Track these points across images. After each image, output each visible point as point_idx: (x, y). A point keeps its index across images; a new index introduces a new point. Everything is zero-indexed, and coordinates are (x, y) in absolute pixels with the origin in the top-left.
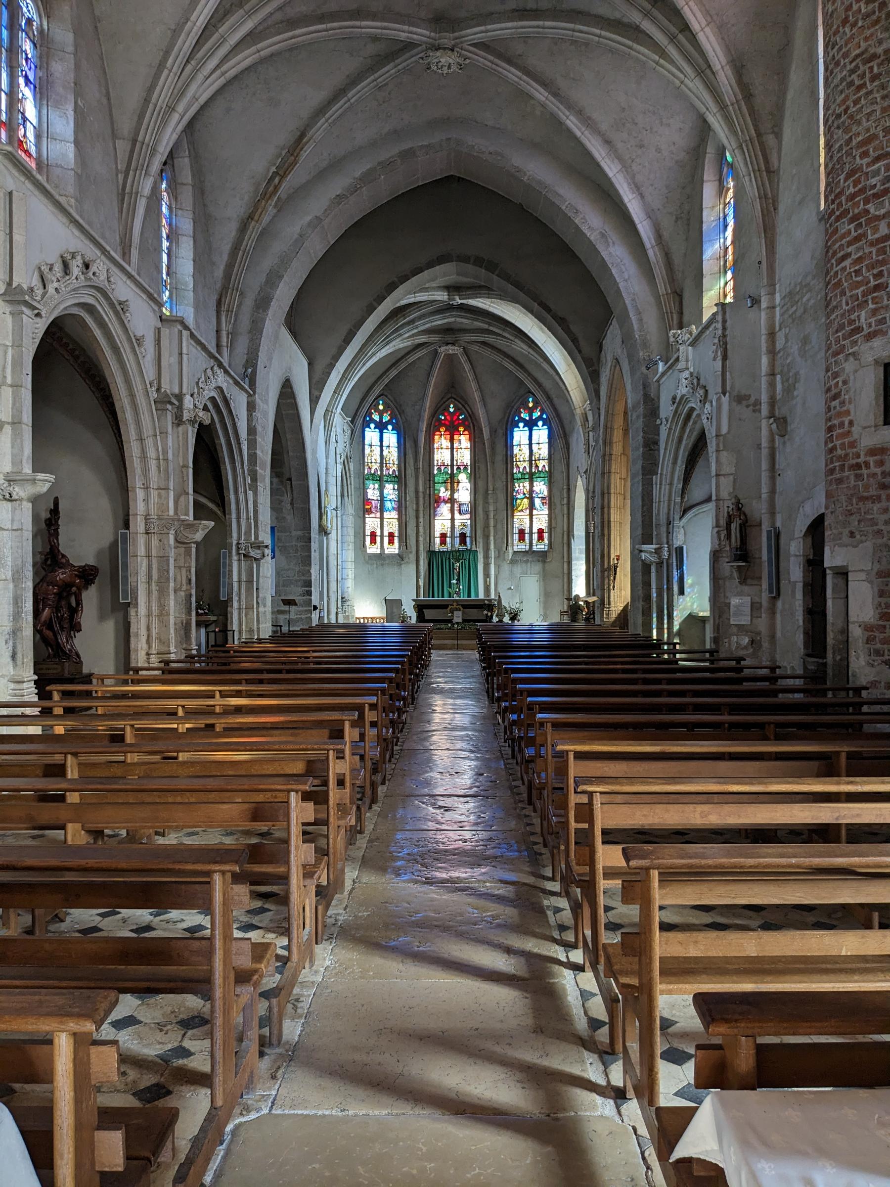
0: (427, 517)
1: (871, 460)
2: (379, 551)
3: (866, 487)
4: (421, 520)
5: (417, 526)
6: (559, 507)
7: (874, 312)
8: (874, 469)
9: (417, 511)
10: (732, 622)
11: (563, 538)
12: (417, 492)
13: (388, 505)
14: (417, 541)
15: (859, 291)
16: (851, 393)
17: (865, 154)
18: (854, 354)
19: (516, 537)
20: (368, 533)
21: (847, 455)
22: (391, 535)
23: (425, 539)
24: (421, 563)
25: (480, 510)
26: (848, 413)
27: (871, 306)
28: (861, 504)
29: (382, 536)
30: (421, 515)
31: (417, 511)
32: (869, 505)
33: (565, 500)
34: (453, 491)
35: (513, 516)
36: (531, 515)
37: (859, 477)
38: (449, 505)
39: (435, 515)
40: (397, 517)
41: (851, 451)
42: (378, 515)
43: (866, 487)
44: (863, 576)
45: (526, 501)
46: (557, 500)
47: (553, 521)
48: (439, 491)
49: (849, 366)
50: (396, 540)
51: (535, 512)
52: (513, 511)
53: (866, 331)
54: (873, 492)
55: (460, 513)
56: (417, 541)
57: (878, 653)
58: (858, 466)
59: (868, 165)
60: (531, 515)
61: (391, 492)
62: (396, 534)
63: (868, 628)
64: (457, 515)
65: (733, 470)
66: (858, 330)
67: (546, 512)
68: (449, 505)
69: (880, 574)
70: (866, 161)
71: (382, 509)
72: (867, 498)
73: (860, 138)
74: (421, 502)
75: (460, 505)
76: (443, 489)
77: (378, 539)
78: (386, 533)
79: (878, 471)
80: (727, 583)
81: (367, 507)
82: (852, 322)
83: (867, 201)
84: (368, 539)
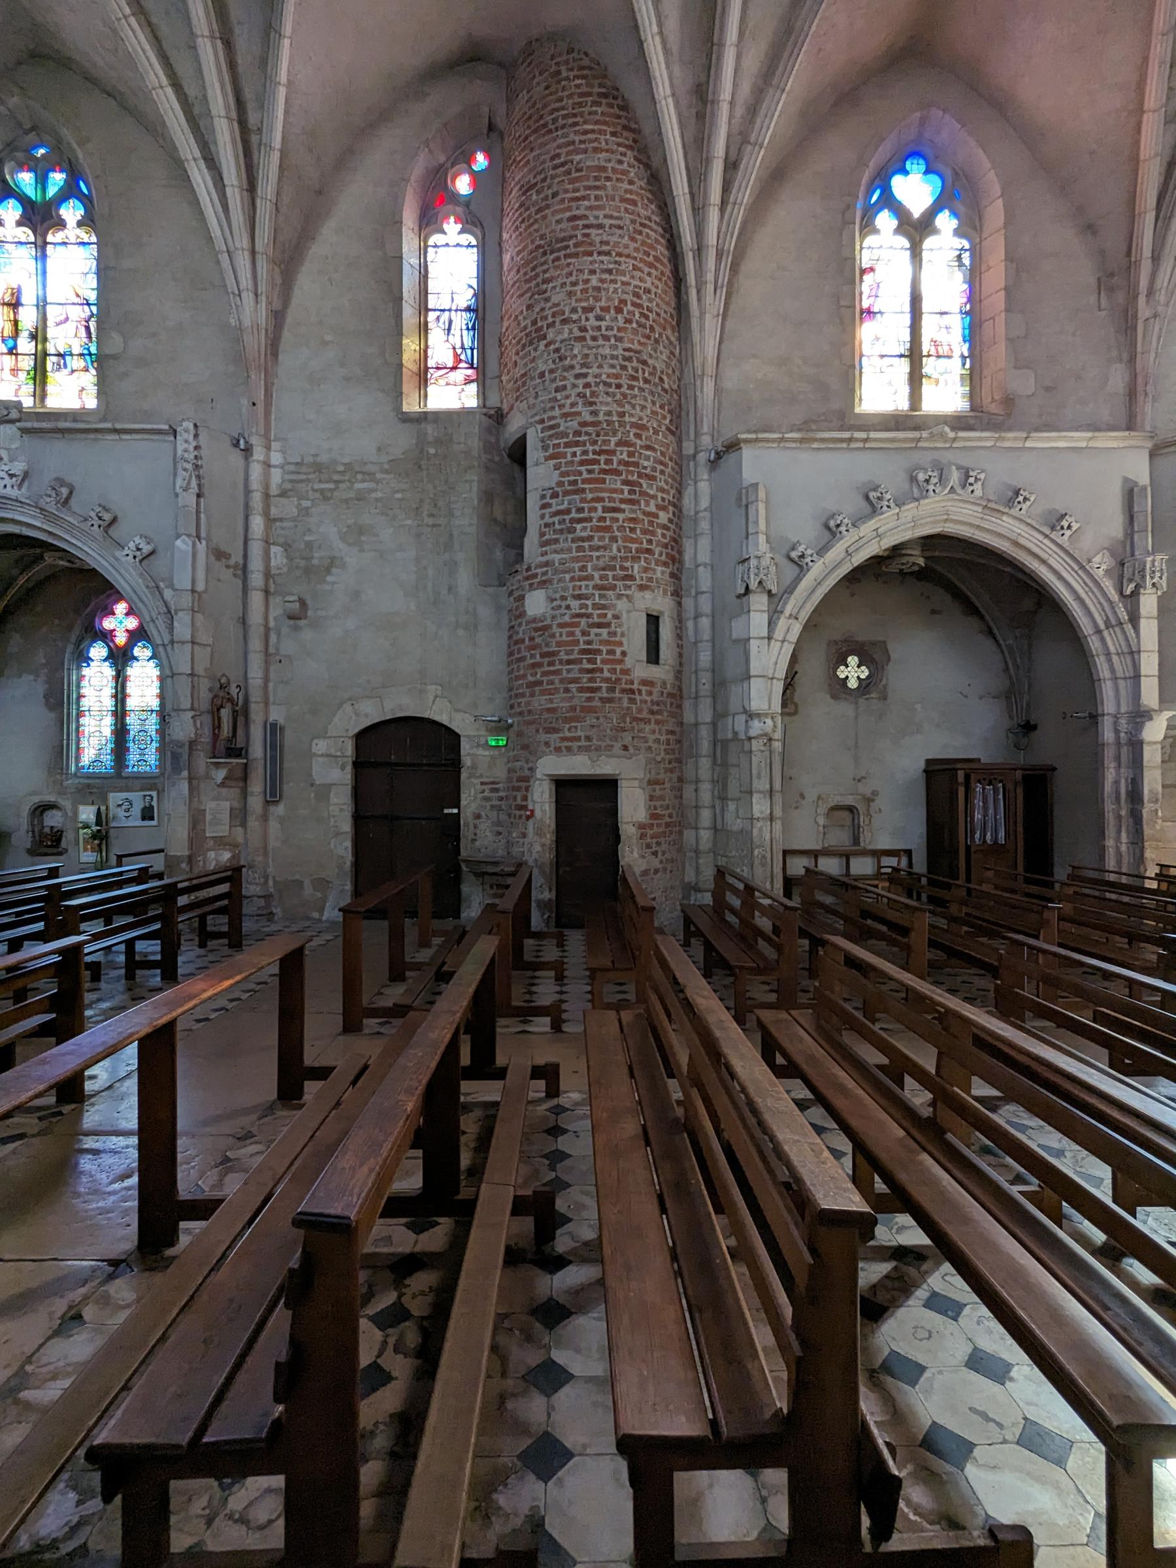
1: (644, 689)
3: (640, 711)
7: (646, 570)
8: (645, 697)
10: (208, 835)
15: (634, 546)
16: (625, 628)
17: (638, 436)
18: (627, 596)
21: (618, 680)
26: (621, 644)
27: (643, 563)
28: (634, 723)
32: (642, 725)
37: (632, 701)
41: (624, 678)
43: (640, 711)
44: (636, 783)
49: (622, 605)
53: (638, 582)
54: (645, 715)
57: (649, 846)
58: (632, 691)
59: (641, 447)
63: (641, 826)
65: (210, 641)
66: (631, 578)
69: (650, 783)
70: (639, 442)
72: (641, 720)
73: (633, 420)
79: (648, 699)
80: (202, 786)
82: (623, 568)
83: (640, 475)
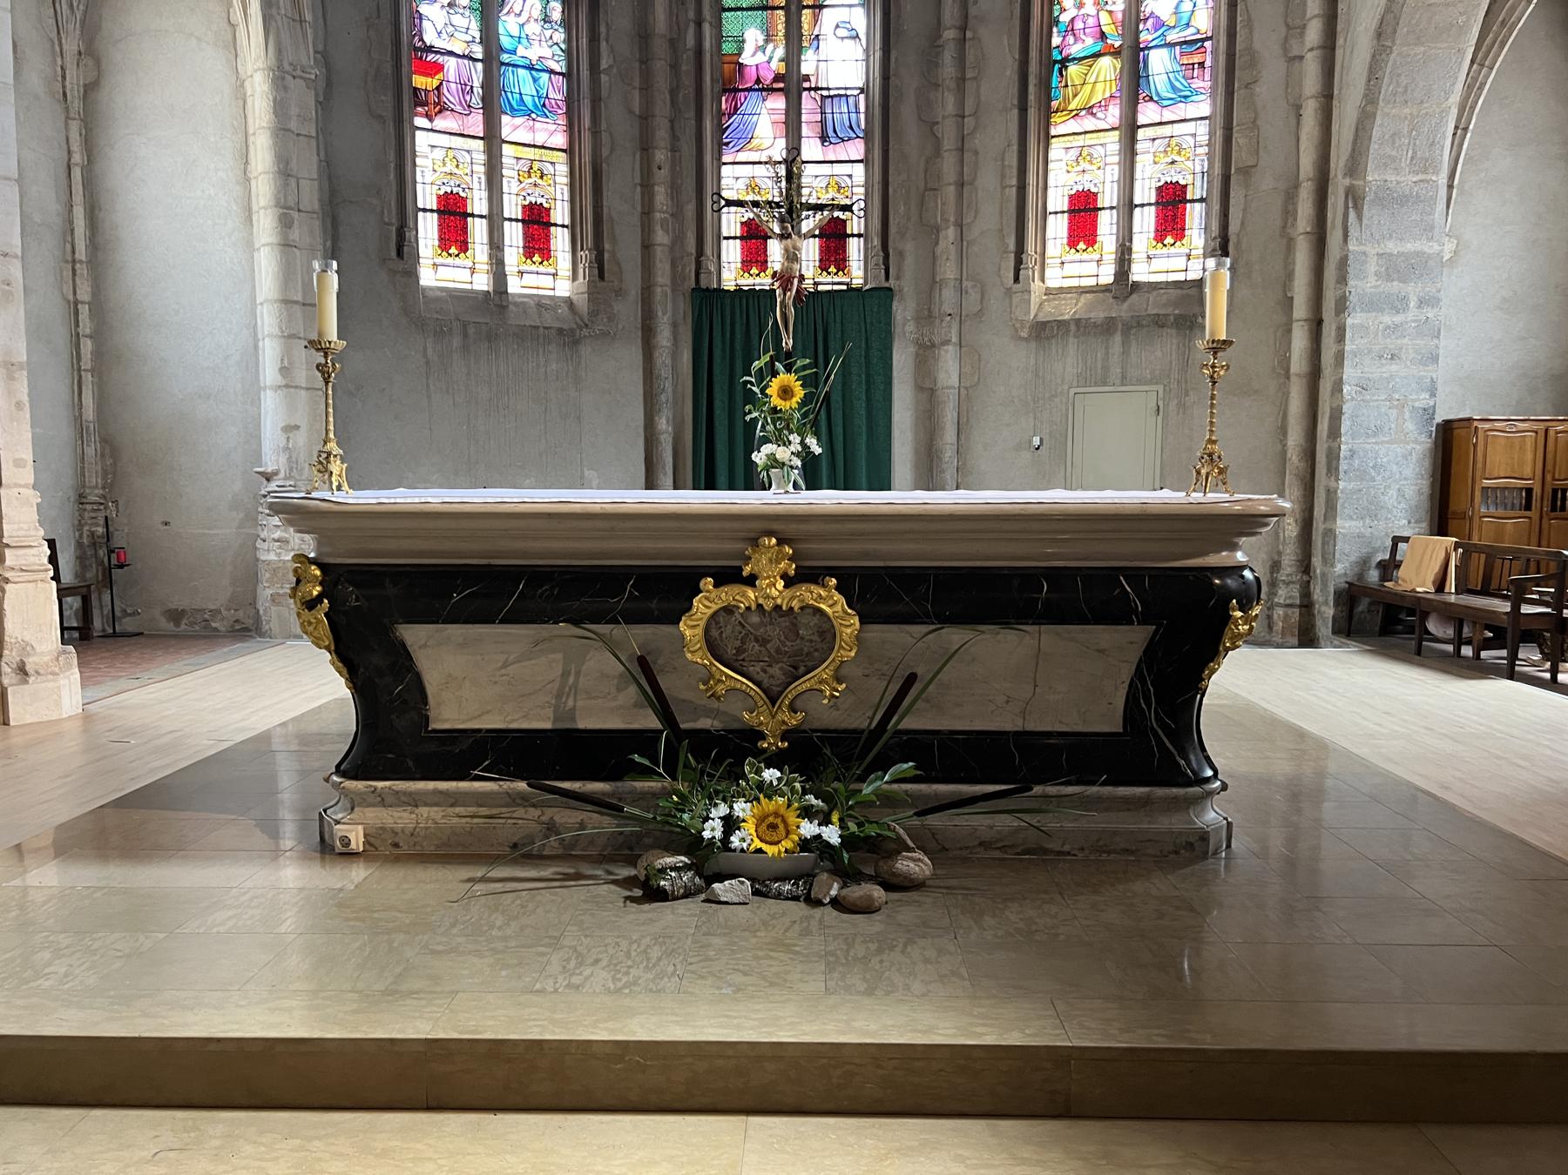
0: (688, 149)
2: (482, 283)
4: (661, 156)
5: (647, 186)
6: (1271, 71)
9: (645, 118)
11: (1289, 212)
12: (644, 36)
13: (521, 84)
14: (647, 247)
19: (1058, 227)
20: (427, 196)
22: (536, 220)
23: (678, 240)
24: (664, 338)
25: (906, 113)
29: (495, 220)
30: (662, 134)
31: (645, 118)
33: (1314, 33)
34: (795, 43)
35: (1048, 138)
36: (1130, 130)
38: (778, 103)
39: (720, 146)
40: (560, 140)
42: (476, 123)
45: (1108, 67)
46: (1265, 38)
47: (1239, 139)
48: (741, 42)
50: (560, 240)
51: (1147, 113)
52: (1047, 114)
55: (824, 138)
56: (647, 247)
60: (1130, 130)
61: (533, 28)
62: (560, 214)
64: (811, 148)
67: (1204, 108)
68: (778, 103)
71: (492, 104)
74: (662, 82)
75: (828, 98)
76: (753, 36)
77: (478, 230)
78: (512, 207)
81: (419, 81)
84: (428, 229)
